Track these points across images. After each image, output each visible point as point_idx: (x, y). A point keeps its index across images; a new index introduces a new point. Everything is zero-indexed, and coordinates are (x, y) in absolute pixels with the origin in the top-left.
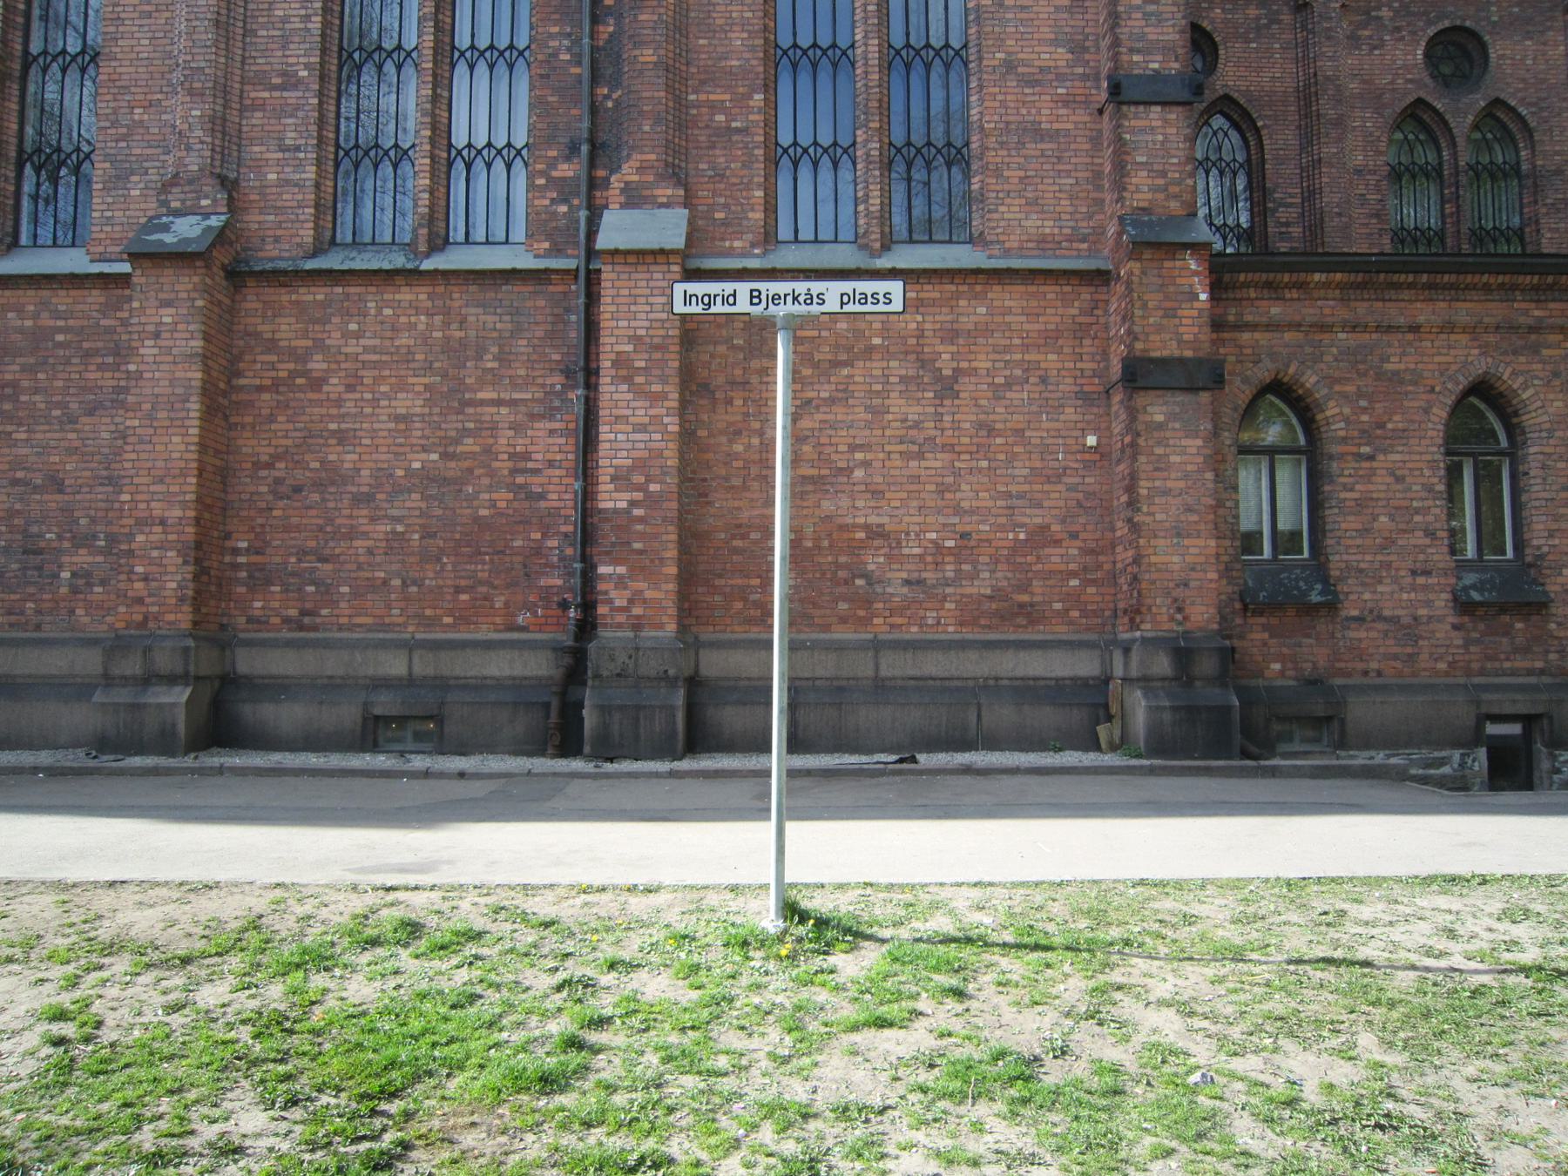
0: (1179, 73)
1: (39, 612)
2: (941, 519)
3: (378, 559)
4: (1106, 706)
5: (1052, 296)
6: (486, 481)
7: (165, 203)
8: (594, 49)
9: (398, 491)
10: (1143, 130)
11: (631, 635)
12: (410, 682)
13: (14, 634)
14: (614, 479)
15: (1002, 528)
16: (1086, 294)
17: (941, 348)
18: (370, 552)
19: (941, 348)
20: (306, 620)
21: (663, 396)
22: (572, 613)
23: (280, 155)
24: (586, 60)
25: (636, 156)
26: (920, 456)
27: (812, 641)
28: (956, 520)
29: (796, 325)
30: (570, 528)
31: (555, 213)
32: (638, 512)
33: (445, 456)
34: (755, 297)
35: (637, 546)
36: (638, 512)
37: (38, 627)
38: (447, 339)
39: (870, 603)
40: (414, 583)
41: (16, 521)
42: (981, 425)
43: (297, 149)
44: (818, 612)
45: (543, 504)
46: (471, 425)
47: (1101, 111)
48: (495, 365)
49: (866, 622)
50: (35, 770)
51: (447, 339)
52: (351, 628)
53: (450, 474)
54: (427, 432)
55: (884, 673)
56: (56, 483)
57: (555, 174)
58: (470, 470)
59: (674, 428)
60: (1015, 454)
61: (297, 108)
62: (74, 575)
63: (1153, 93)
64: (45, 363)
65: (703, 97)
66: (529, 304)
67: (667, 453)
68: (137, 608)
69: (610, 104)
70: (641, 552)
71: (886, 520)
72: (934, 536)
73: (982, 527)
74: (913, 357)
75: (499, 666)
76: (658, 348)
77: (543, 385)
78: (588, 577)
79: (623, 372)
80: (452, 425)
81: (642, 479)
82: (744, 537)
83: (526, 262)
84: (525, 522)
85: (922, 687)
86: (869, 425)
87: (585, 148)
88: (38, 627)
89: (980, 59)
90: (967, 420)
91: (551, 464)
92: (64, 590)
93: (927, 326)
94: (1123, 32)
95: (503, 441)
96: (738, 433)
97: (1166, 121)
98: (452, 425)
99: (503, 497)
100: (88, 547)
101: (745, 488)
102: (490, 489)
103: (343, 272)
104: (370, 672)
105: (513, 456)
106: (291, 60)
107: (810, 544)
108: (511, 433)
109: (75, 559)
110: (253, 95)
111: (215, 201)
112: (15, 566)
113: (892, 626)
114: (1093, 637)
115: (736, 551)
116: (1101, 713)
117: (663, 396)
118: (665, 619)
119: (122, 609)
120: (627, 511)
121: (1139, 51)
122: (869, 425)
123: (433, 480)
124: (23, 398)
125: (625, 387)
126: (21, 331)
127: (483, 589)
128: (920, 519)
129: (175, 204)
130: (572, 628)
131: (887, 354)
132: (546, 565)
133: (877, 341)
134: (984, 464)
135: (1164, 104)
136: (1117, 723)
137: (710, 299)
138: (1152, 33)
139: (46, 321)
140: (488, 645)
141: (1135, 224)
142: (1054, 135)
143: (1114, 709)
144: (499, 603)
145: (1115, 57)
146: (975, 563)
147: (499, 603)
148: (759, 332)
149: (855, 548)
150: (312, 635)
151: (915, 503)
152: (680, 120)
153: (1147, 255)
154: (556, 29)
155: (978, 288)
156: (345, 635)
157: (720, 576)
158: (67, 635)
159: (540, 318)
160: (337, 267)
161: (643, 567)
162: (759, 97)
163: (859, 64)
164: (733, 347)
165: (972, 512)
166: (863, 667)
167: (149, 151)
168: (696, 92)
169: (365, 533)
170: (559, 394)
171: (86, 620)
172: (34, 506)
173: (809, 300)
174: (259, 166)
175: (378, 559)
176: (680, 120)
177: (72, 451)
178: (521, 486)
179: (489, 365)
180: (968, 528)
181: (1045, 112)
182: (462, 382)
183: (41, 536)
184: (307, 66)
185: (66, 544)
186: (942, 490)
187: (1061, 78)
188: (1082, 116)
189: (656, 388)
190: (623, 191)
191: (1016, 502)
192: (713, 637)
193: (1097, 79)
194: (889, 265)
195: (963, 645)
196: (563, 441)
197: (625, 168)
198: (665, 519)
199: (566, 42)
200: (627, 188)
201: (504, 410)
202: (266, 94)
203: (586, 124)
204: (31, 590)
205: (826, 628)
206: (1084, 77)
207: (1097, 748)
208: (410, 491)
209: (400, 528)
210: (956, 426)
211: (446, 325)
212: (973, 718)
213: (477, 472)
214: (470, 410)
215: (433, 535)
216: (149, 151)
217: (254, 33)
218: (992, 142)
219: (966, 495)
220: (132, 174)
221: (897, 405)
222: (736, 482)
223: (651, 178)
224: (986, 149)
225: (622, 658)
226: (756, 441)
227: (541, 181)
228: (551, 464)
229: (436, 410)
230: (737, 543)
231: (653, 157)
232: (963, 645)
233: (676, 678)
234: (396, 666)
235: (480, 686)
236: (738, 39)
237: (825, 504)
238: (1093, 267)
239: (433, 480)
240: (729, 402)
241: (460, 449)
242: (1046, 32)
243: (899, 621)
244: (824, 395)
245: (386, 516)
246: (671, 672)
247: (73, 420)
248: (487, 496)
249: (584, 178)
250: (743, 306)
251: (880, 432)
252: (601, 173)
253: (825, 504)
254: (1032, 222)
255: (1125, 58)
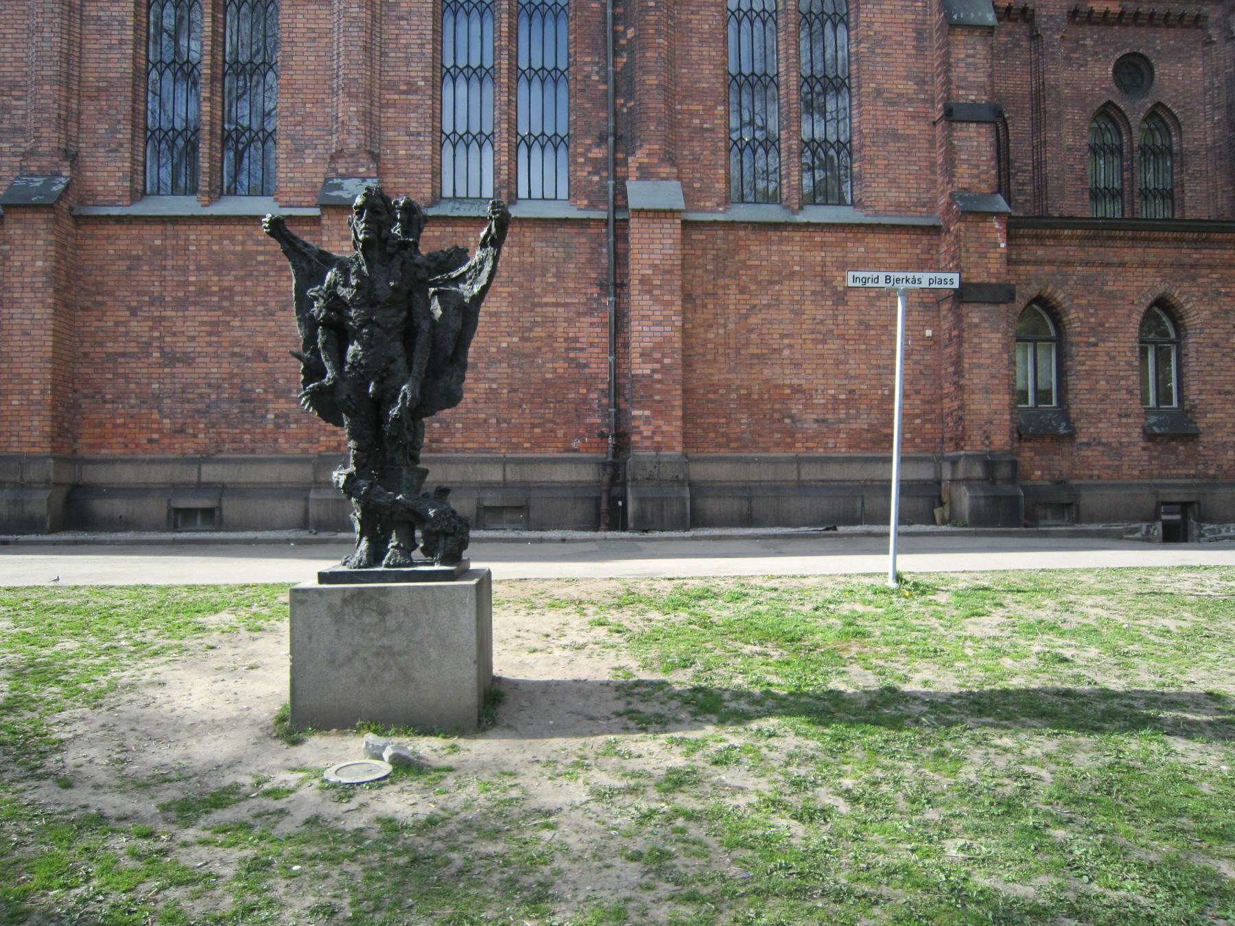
0: (987, 102)
1: (253, 441)
2: (837, 382)
3: (480, 406)
4: (940, 497)
5: (904, 241)
6: (550, 355)
7: (335, 170)
8: (615, 73)
9: (492, 361)
10: (965, 139)
11: (653, 453)
12: (504, 485)
13: (237, 456)
14: (642, 355)
15: (874, 387)
16: (925, 240)
17: (836, 274)
18: (475, 401)
19: (836, 274)
20: (434, 445)
21: (672, 303)
22: (610, 440)
23: (407, 138)
24: (611, 81)
25: (646, 146)
26: (824, 342)
27: (760, 458)
28: (846, 382)
29: (906, 293)
30: (605, 386)
31: (590, 182)
32: (657, 376)
33: (523, 339)
34: (887, 279)
35: (657, 398)
36: (657, 376)
37: (253, 451)
38: (522, 263)
39: (794, 434)
40: (505, 421)
41: (235, 381)
42: (861, 323)
43: (419, 134)
44: (761, 440)
45: (587, 370)
46: (539, 319)
47: (934, 123)
48: (554, 280)
49: (790, 446)
50: (288, 541)
51: (522, 263)
52: (464, 450)
53: (526, 351)
54: (511, 323)
55: (804, 477)
56: (262, 356)
57: (590, 155)
58: (539, 349)
59: (679, 324)
60: (882, 341)
61: (418, 107)
62: (277, 416)
63: (971, 114)
64: (251, 275)
65: (685, 107)
66: (575, 240)
67: (675, 339)
68: (333, 438)
69: (625, 110)
70: (660, 402)
71: (803, 382)
72: (832, 392)
73: (862, 387)
74: (819, 279)
75: (562, 474)
76: (667, 272)
77: (585, 294)
78: (620, 416)
79: (646, 288)
80: (527, 319)
81: (659, 356)
82: (715, 392)
83: (573, 213)
84: (576, 382)
85: (827, 486)
86: (792, 322)
87: (611, 139)
88: (253, 451)
89: (859, 87)
90: (853, 319)
91: (592, 345)
92: (270, 426)
93: (828, 259)
94: (953, 75)
95: (560, 330)
96: (710, 326)
97: (979, 133)
98: (527, 319)
99: (561, 366)
100: (287, 398)
101: (715, 361)
102: (553, 360)
103: (453, 218)
104: (479, 478)
105: (567, 339)
106: (413, 74)
107: (756, 397)
108: (566, 324)
109: (277, 406)
110: (387, 97)
111: (368, 169)
112: (236, 411)
113: (807, 448)
114: (929, 455)
115: (713, 401)
116: (936, 501)
117: (672, 303)
118: (675, 444)
119: (323, 438)
120: (650, 376)
121: (963, 88)
122: (792, 322)
123: (515, 355)
124: (237, 299)
125: (647, 297)
126: (234, 253)
127: (549, 425)
128: (824, 381)
129: (341, 171)
130: (611, 450)
131: (803, 276)
132: (590, 410)
133: (797, 268)
134: (863, 347)
135: (978, 122)
136: (947, 507)
137: (866, 280)
138: (971, 77)
139: (250, 247)
140: (554, 461)
141: (962, 198)
142: (905, 138)
143: (945, 498)
144: (560, 434)
145: (948, 91)
146: (858, 409)
147: (560, 434)
148: (889, 295)
149: (784, 400)
150: (439, 455)
151: (821, 371)
152: (672, 122)
153: (970, 219)
154: (588, 59)
155: (859, 235)
156: (459, 455)
157: (700, 417)
158: (273, 456)
159: (582, 250)
160: (450, 214)
161: (661, 411)
162: (721, 108)
163: (782, 87)
164: (706, 271)
165: (856, 377)
166: (789, 473)
167: (318, 133)
168: (680, 103)
169: (472, 389)
170: (597, 300)
171: (286, 446)
172: (247, 371)
173: (914, 282)
174: (393, 145)
175: (480, 406)
176: (672, 122)
177: (272, 334)
178: (573, 359)
179: (550, 280)
180: (853, 387)
181: (901, 123)
182: (532, 290)
183: (252, 390)
184: (424, 78)
185: (270, 396)
186: (838, 363)
187: (910, 101)
188: (923, 126)
189: (667, 298)
190: (638, 168)
191: (882, 371)
192: (696, 455)
193: (933, 102)
194: (805, 220)
195: (851, 460)
196: (599, 330)
197: (639, 153)
198: (674, 381)
199: (596, 68)
200: (640, 167)
201: (560, 310)
202: (397, 97)
203: (611, 124)
204: (247, 426)
205: (767, 449)
206: (925, 100)
207: (934, 523)
208: (500, 362)
209: (494, 386)
210: (846, 323)
211: (521, 253)
212: (859, 505)
213: (544, 350)
214: (539, 309)
215: (516, 391)
216: (318, 133)
217: (386, 55)
218: (867, 141)
219: (852, 367)
220: (307, 148)
221: (809, 308)
222: (710, 357)
223: (656, 161)
224: (862, 146)
225: (650, 468)
226: (721, 331)
227: (581, 160)
228: (592, 345)
229: (516, 309)
230: (711, 396)
231: (657, 147)
232: (851, 460)
233: (684, 481)
234: (494, 474)
235: (550, 487)
236: (707, 70)
237: (766, 372)
238: (931, 223)
239: (515, 355)
240: (705, 306)
241: (532, 335)
242: (902, 71)
243: (811, 445)
244: (764, 302)
245: (485, 378)
246: (681, 477)
247: (272, 314)
248: (550, 365)
249: (611, 157)
250: (882, 283)
251: (798, 326)
252: (620, 156)
253: (766, 372)
254: (893, 194)
255: (954, 92)
